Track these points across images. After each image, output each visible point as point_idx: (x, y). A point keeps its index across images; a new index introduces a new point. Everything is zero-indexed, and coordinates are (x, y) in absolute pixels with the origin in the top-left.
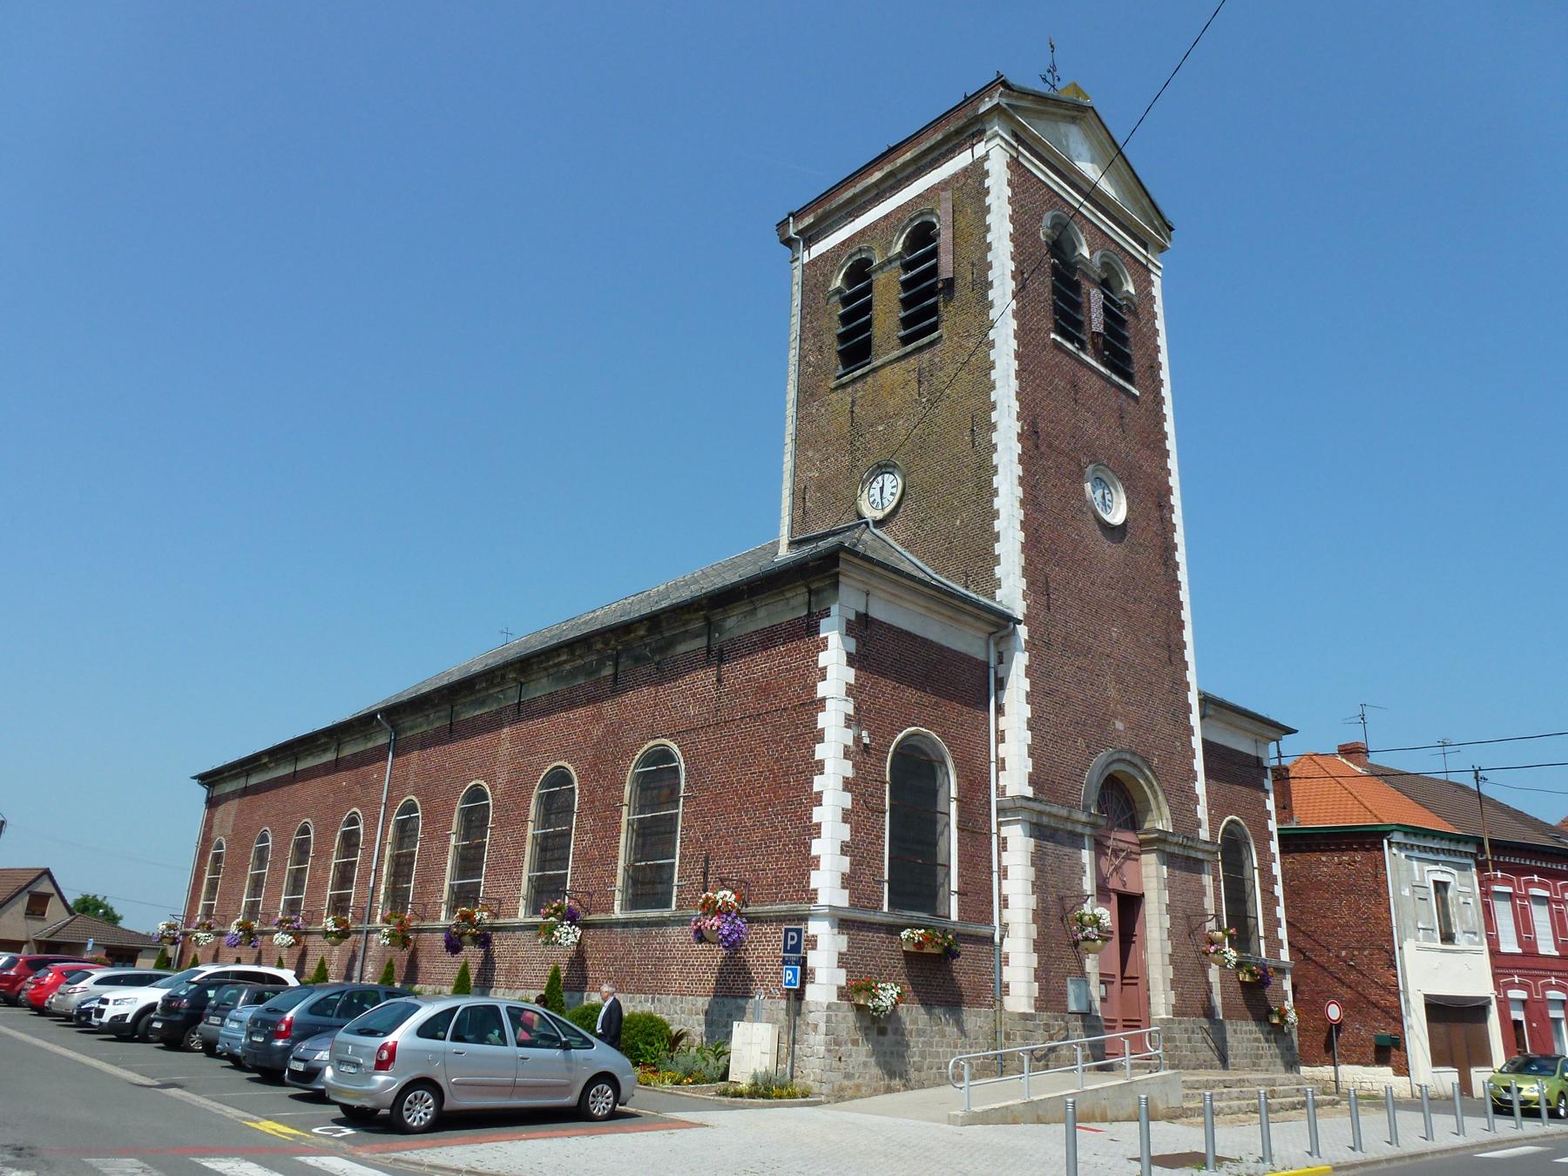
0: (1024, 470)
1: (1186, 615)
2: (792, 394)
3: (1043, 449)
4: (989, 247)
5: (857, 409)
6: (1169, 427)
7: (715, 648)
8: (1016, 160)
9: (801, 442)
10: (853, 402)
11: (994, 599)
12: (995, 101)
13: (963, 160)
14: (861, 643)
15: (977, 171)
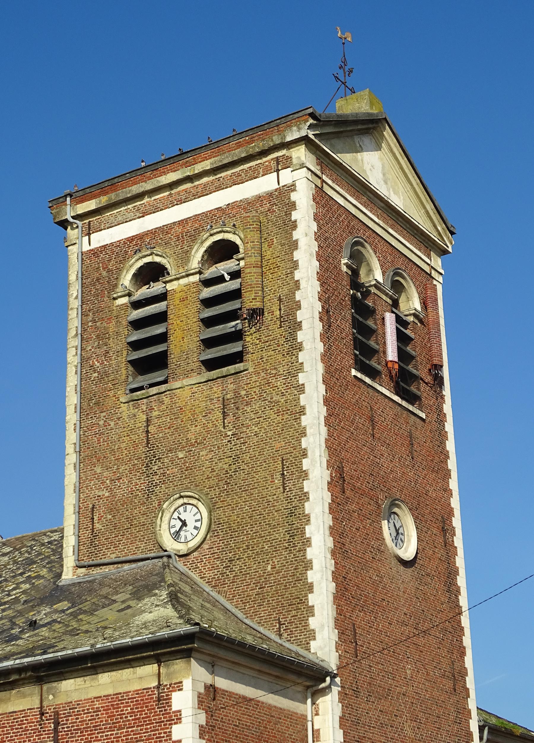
0: (334, 519)
1: (467, 641)
2: (72, 399)
3: (348, 493)
4: (297, 285)
5: (151, 429)
6: (450, 445)
7: (50, 712)
8: (321, 189)
9: (90, 455)
10: (148, 421)
11: (308, 650)
12: (303, 133)
13: (266, 184)
14: (210, 713)
15: (282, 198)
